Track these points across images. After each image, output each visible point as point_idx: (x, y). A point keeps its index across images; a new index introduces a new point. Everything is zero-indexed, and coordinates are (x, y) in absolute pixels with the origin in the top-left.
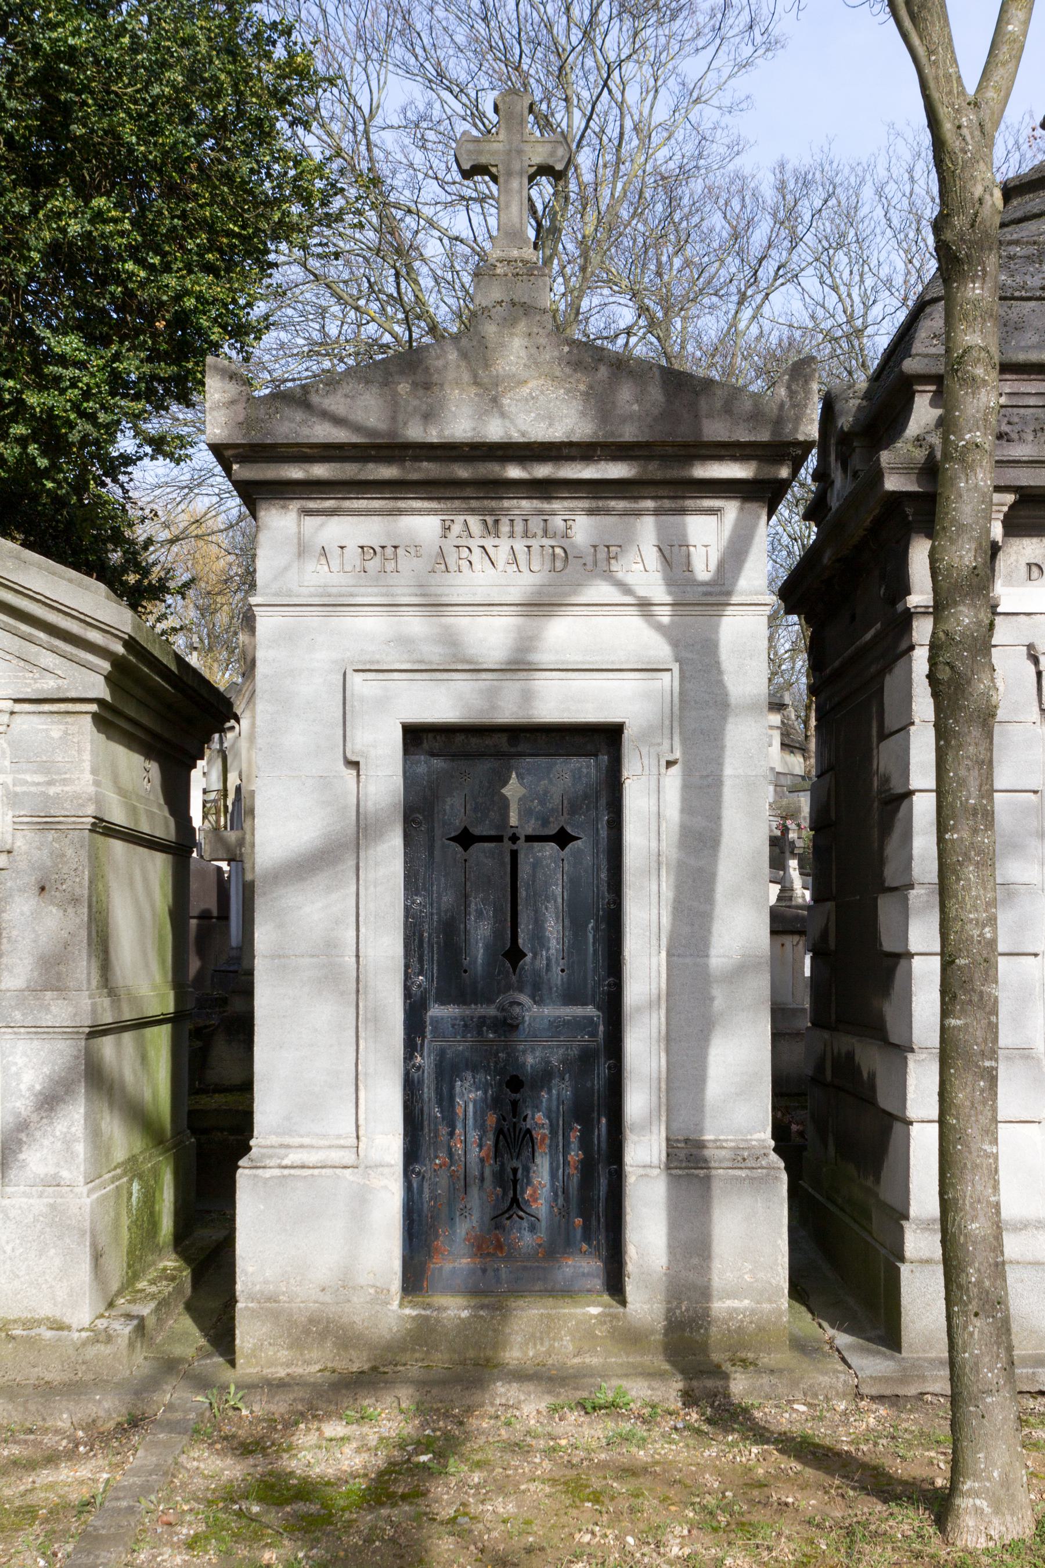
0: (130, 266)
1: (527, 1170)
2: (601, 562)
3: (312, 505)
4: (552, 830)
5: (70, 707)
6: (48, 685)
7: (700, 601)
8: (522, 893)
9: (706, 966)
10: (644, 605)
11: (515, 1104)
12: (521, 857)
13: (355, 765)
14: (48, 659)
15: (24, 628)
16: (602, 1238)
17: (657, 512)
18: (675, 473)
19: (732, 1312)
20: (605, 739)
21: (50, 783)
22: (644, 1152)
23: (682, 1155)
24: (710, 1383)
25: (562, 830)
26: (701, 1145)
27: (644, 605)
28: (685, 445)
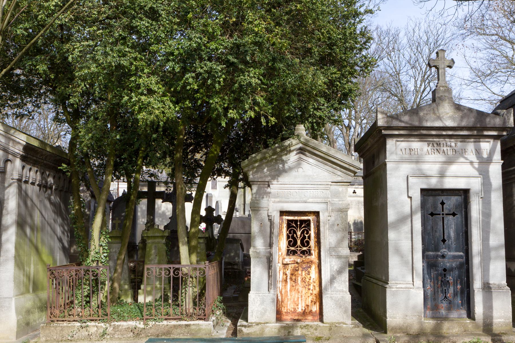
0: (338, 83)
1: (448, 290)
2: (462, 153)
3: (398, 139)
4: (451, 212)
5: (344, 184)
6: (339, 179)
7: (485, 162)
8: (445, 227)
9: (489, 243)
10: (471, 163)
11: (445, 275)
12: (445, 219)
13: (411, 198)
14: (339, 173)
15: (334, 166)
16: (466, 305)
17: (475, 142)
18: (480, 134)
19: (499, 322)
20: (465, 193)
21: (339, 201)
22: (477, 284)
23: (486, 286)
24: (498, 338)
25: (454, 212)
26: (489, 284)
27: (471, 163)
28: (484, 127)
